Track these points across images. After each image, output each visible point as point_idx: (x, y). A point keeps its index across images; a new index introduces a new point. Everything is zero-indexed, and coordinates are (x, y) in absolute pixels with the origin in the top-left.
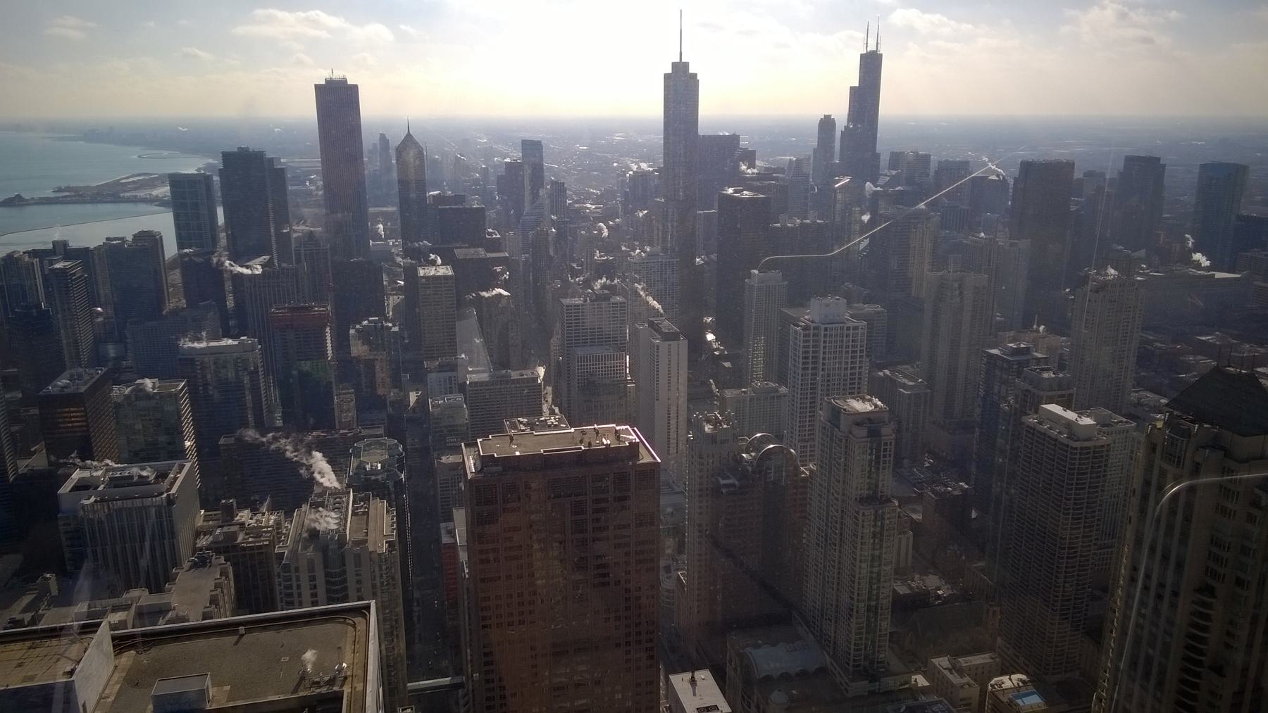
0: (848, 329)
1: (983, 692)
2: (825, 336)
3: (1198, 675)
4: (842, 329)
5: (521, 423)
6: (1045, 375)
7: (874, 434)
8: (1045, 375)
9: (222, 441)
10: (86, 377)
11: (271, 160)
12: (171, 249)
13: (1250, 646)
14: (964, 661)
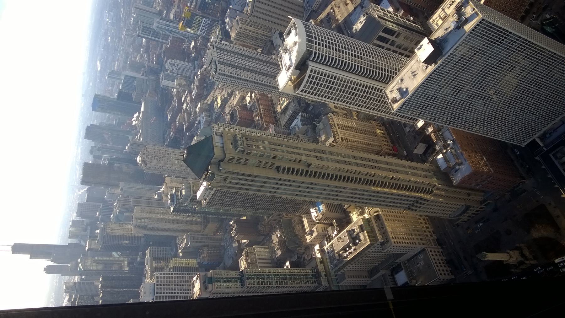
0: (157, 281)
1: (318, 223)
2: (161, 293)
3: (311, 172)
6: (184, 193)
7: (211, 280)
8: (184, 193)
13: (299, 154)
14: (307, 230)
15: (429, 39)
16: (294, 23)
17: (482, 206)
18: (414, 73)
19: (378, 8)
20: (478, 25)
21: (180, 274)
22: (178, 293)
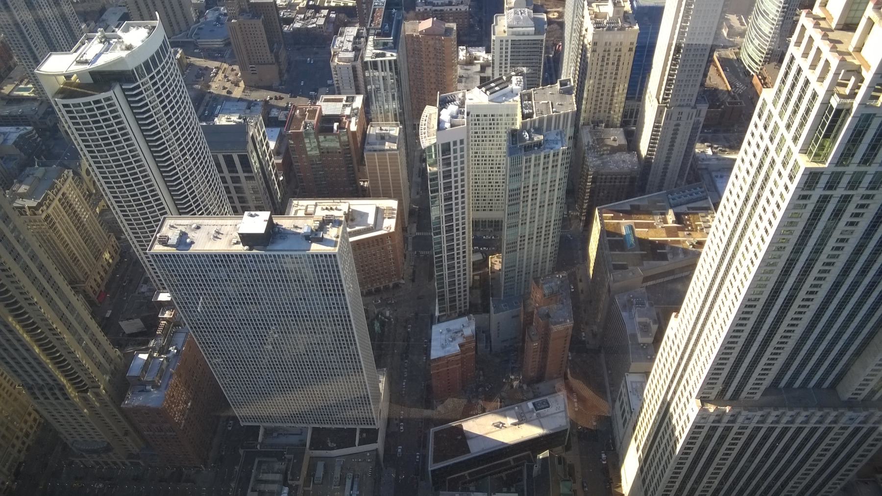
15: (271, 219)
16: (154, 27)
17: (127, 462)
18: (219, 234)
19: (262, 128)
20: (326, 256)
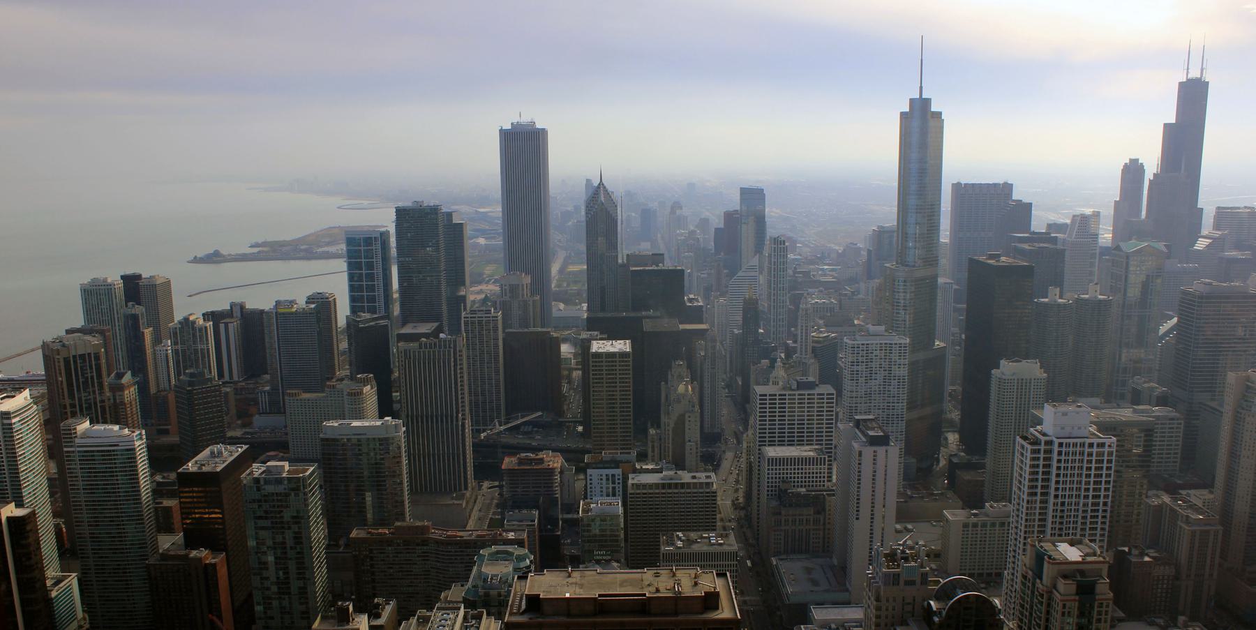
0: (1091, 445)
2: (1060, 453)
4: (1083, 445)
5: (680, 539)
9: (354, 534)
10: (225, 454)
11: (449, 215)
12: (343, 311)
21: (1105, 504)
22: (1056, 496)
